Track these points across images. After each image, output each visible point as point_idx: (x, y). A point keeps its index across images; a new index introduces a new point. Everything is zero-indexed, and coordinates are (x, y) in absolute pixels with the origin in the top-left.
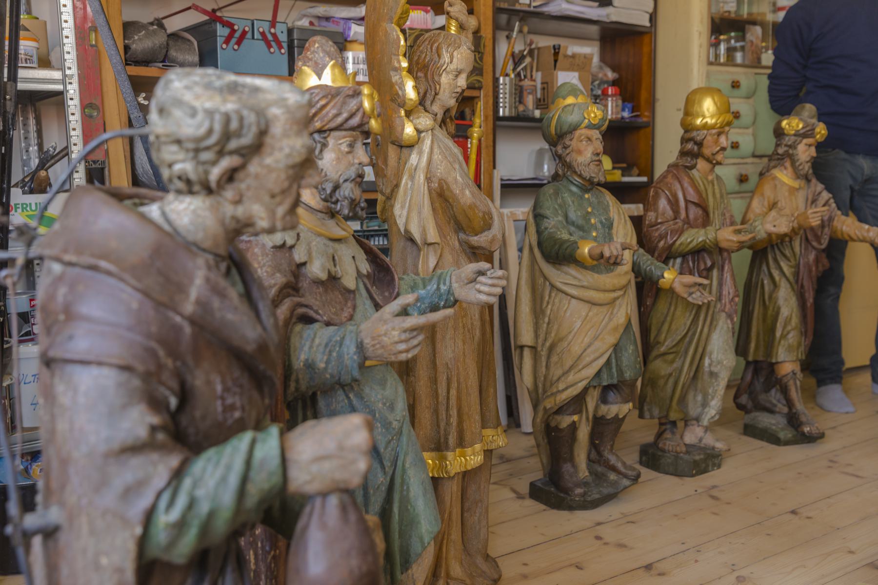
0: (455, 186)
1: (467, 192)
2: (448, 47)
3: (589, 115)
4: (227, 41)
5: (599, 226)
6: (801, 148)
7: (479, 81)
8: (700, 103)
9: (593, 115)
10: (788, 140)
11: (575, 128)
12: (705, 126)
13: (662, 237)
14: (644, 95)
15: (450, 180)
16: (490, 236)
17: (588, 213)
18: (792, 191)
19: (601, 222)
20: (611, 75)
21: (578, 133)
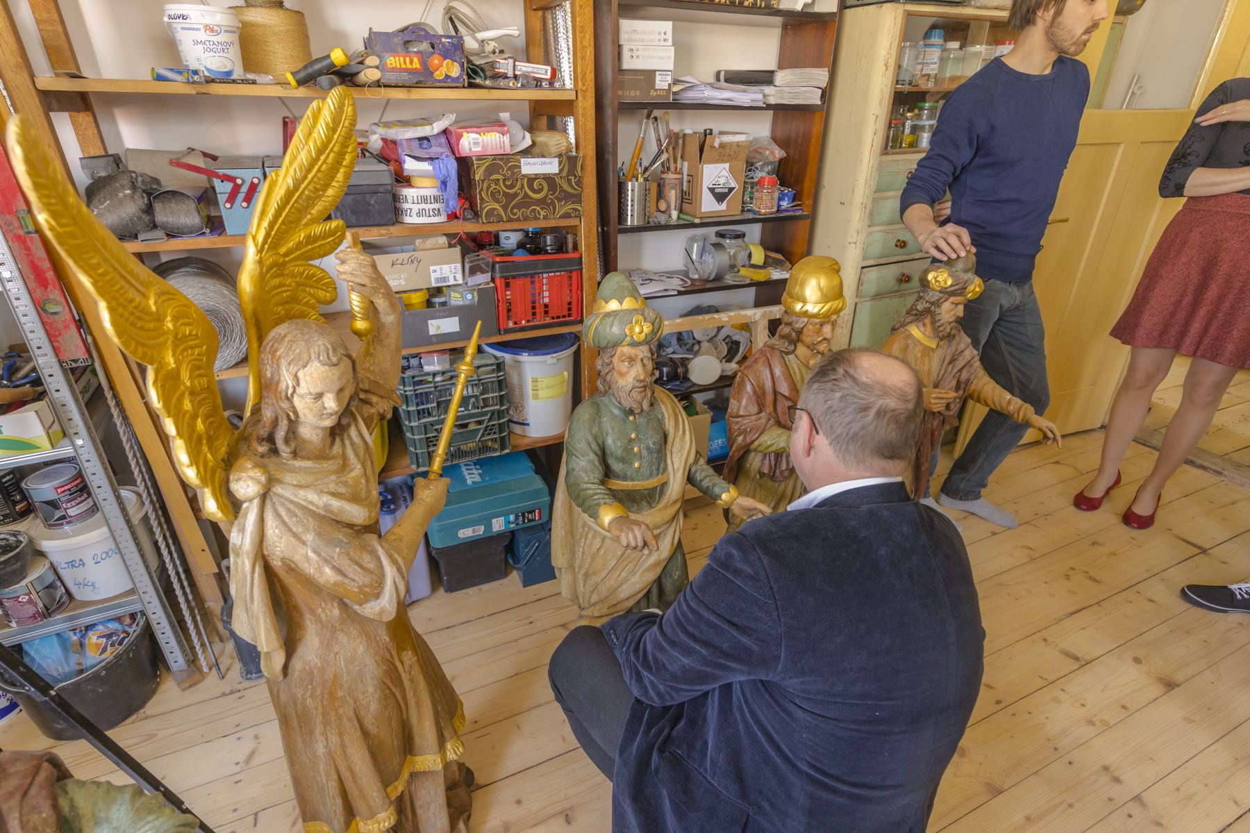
0: (306, 565)
1: (327, 570)
2: (289, 364)
3: (631, 329)
4: (232, 198)
5: (645, 453)
6: (946, 306)
7: (576, 210)
8: (803, 285)
9: (637, 329)
10: (932, 296)
11: (616, 345)
12: (805, 314)
13: (744, 433)
14: (807, 185)
15: (297, 558)
16: (377, 610)
17: (631, 440)
18: (927, 351)
19: (648, 449)
20: (779, 153)
21: (619, 350)
